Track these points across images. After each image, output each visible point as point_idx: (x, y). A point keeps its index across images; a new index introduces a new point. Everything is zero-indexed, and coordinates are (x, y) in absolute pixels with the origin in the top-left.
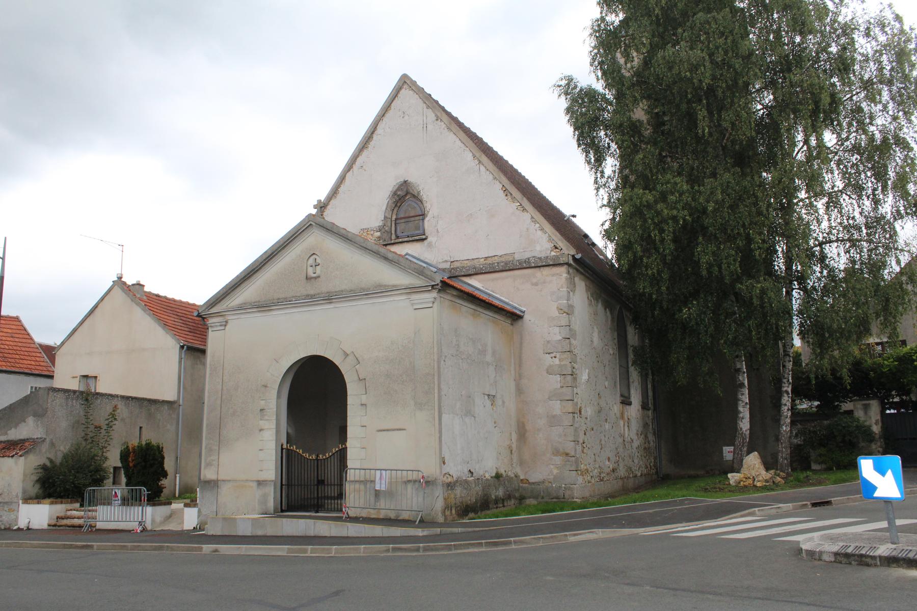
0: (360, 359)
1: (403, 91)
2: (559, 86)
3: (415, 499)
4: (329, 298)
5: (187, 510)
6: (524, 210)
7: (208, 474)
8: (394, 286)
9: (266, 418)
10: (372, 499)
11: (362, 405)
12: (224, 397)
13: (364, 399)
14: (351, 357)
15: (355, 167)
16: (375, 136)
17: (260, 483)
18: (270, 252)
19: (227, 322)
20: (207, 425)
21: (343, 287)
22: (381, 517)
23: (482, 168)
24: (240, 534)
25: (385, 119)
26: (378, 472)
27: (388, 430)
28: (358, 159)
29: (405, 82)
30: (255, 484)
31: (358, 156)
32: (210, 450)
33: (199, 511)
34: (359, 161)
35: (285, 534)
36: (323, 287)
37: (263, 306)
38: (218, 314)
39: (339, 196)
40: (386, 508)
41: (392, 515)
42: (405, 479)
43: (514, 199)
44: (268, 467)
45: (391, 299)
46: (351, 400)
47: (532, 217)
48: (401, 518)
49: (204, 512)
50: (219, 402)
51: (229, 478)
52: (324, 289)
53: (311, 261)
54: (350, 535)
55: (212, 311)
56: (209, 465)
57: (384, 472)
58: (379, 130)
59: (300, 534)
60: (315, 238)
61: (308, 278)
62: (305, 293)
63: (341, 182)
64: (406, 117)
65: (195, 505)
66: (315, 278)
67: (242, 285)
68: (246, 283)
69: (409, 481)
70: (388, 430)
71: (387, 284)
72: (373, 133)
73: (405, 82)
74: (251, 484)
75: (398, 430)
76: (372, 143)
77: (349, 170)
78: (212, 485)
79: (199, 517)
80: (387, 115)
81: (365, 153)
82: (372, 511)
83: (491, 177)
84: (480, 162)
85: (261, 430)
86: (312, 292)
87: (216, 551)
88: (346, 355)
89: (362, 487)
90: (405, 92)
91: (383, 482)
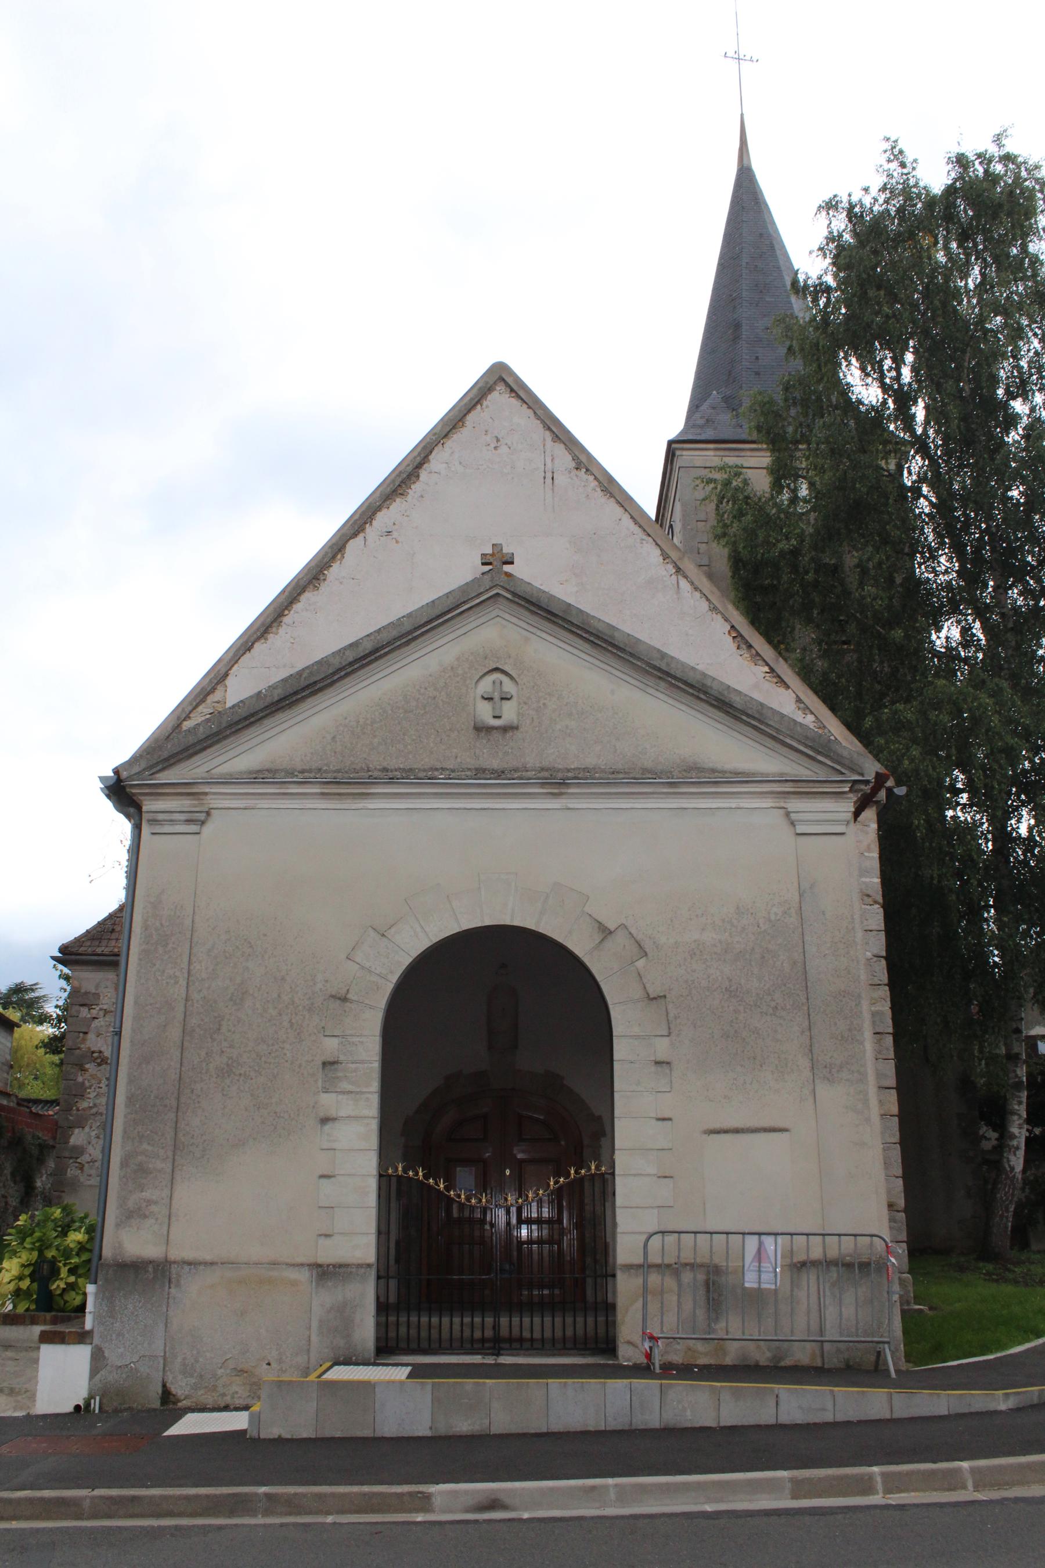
0: (648, 946)
1: (494, 396)
2: (710, 481)
3: (831, 1313)
4: (557, 781)
5: (49, 1353)
6: (782, 682)
7: (128, 1240)
8: (737, 774)
9: (345, 1086)
10: (701, 1314)
11: (658, 1063)
12: (193, 1021)
13: (662, 1048)
14: (620, 940)
15: (372, 532)
16: (423, 474)
17: (326, 1273)
18: (368, 646)
19: (208, 814)
20: (130, 1100)
21: (590, 761)
22: (728, 1361)
23: (683, 583)
24: (389, 1428)
25: (449, 443)
26: (752, 1243)
27: (737, 1131)
28: (380, 515)
29: (499, 380)
30: (303, 1276)
31: (379, 509)
32: (139, 1173)
33: (98, 1360)
34: (382, 519)
35: (556, 1426)
36: (530, 753)
37: (344, 779)
38: (186, 790)
39: (324, 587)
40: (740, 1335)
41: (762, 1356)
42: (801, 1257)
43: (757, 657)
44: (353, 1227)
45: (733, 803)
46: (621, 1050)
47: (799, 700)
48: (787, 1362)
49: (114, 1356)
50: (175, 1033)
51: (208, 1258)
52: (532, 760)
53: (486, 685)
54: (784, 1419)
55: (165, 777)
56: (132, 1215)
57: (769, 1242)
58: (437, 460)
59: (620, 1428)
60: (495, 632)
61: (481, 729)
62: (472, 763)
63: (333, 558)
64: (503, 450)
65: (83, 1337)
66: (505, 729)
67: (268, 722)
68: (280, 716)
69: (803, 1264)
70: (737, 1131)
71: (719, 766)
72: (419, 466)
73: (499, 380)
74: (293, 1274)
75: (766, 1130)
76: (416, 488)
77: (355, 535)
78: (151, 1276)
79: (94, 1371)
80: (456, 437)
81: (397, 506)
82: (700, 1346)
83: (704, 605)
84: (678, 570)
85: (325, 1120)
86: (495, 764)
87: (494, 1504)
88: (605, 932)
89: (670, 1282)
90: (499, 398)
91: (767, 1266)
